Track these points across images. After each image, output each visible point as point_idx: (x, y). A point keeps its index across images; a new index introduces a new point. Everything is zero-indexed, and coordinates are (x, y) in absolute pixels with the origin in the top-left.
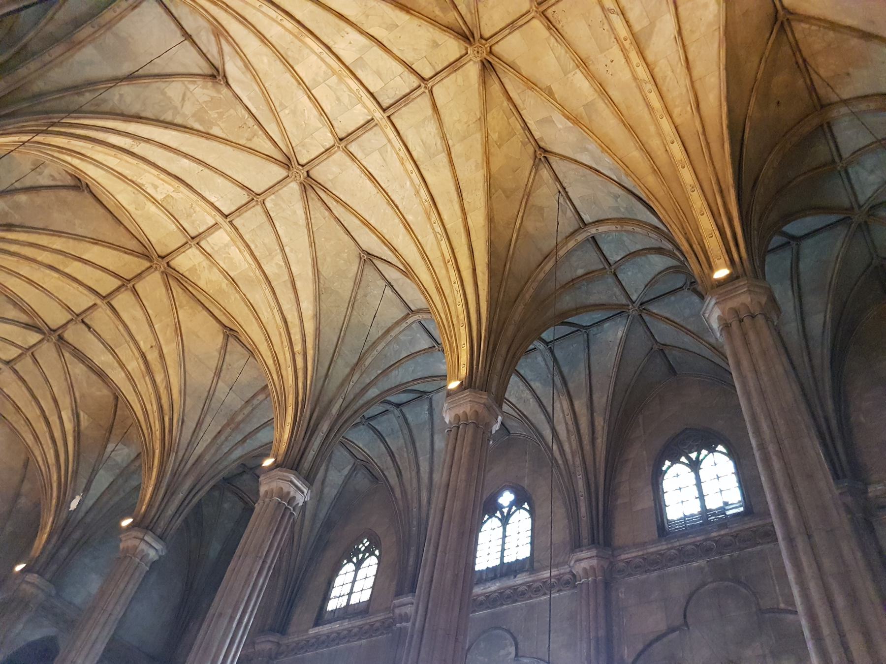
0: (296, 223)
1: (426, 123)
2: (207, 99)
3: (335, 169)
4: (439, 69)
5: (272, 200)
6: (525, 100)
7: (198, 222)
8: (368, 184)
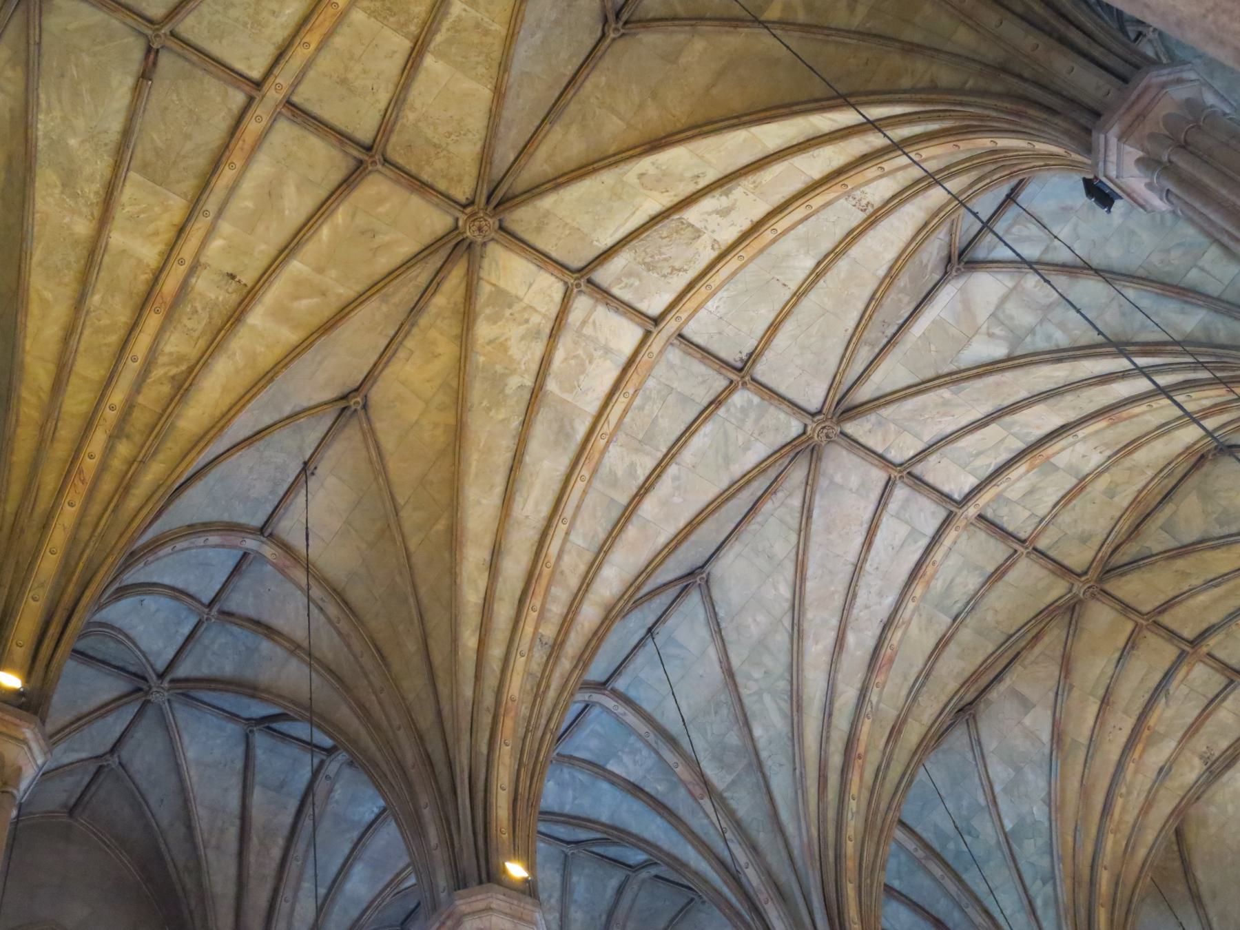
0: (727, 460)
1: (977, 572)
2: (925, 261)
3: (854, 481)
4: (1052, 553)
5: (750, 402)
6: (1037, 663)
7: (637, 283)
8: (859, 540)
